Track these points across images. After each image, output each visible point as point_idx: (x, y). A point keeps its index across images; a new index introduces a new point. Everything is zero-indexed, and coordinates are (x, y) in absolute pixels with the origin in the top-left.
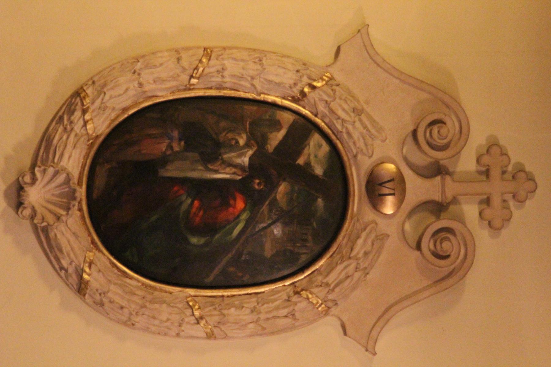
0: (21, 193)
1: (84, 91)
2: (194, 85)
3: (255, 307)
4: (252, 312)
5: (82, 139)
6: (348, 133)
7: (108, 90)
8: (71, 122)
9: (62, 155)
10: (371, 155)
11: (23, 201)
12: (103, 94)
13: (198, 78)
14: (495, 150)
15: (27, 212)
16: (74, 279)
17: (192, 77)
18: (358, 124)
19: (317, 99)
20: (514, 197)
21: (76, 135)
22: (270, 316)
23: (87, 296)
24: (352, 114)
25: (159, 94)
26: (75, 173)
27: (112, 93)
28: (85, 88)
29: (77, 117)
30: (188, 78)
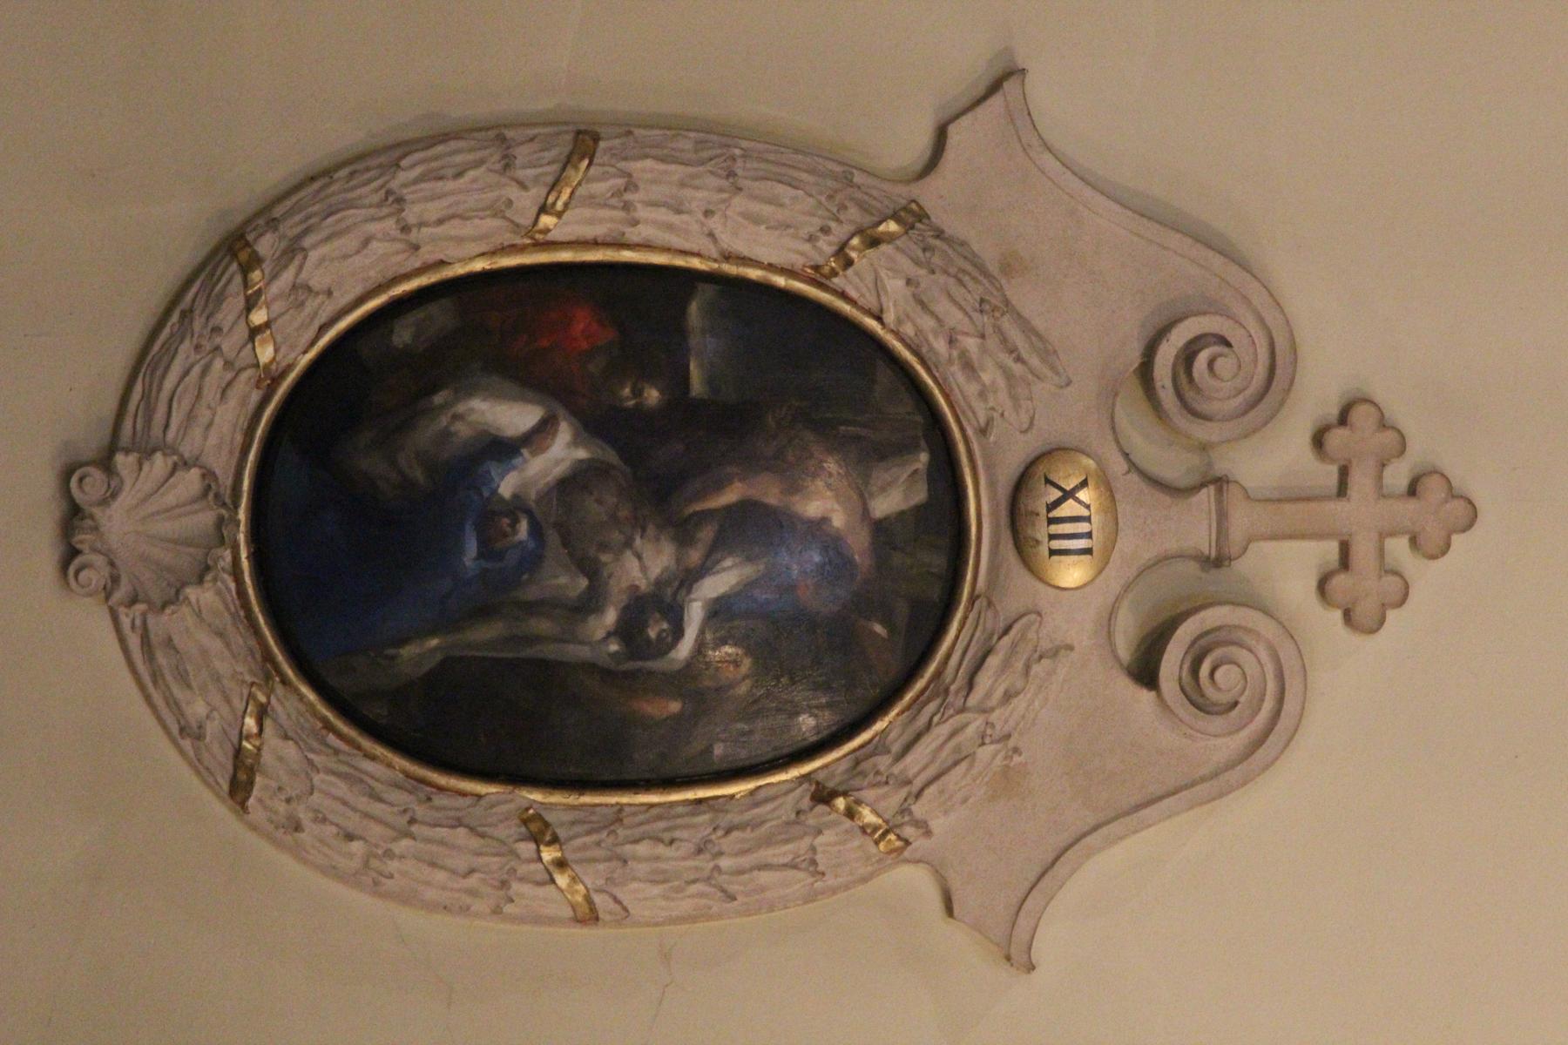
0: (76, 522)
1: (248, 244)
2: (547, 231)
3: (707, 841)
4: (700, 851)
5: (245, 376)
6: (969, 367)
7: (314, 246)
8: (217, 330)
9: (190, 416)
10: (1025, 426)
11: (78, 546)
12: (299, 257)
13: (559, 215)
14: (1360, 414)
15: (95, 577)
16: (220, 757)
17: (543, 209)
18: (993, 342)
19: (883, 273)
20: (1414, 541)
21: (228, 364)
22: (746, 861)
23: (251, 801)
24: (976, 315)
25: (451, 252)
26: (222, 465)
27: (325, 249)
28: (250, 237)
29: (231, 318)
30: (535, 210)
